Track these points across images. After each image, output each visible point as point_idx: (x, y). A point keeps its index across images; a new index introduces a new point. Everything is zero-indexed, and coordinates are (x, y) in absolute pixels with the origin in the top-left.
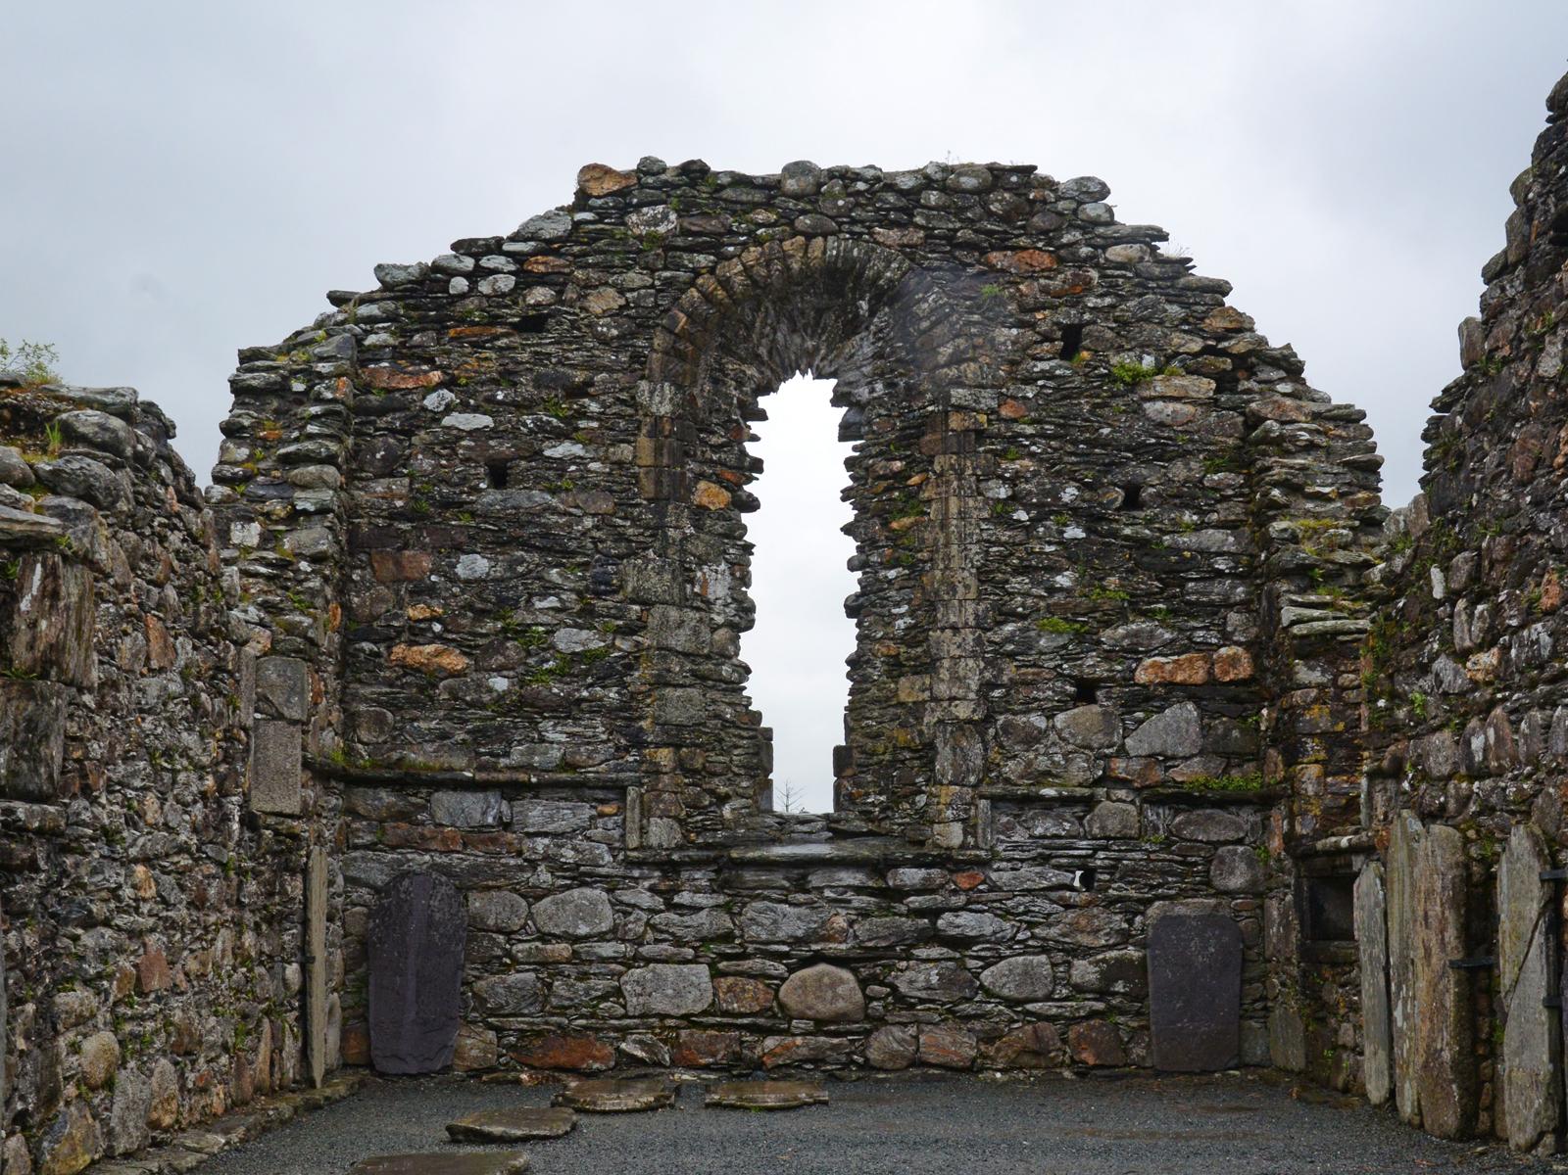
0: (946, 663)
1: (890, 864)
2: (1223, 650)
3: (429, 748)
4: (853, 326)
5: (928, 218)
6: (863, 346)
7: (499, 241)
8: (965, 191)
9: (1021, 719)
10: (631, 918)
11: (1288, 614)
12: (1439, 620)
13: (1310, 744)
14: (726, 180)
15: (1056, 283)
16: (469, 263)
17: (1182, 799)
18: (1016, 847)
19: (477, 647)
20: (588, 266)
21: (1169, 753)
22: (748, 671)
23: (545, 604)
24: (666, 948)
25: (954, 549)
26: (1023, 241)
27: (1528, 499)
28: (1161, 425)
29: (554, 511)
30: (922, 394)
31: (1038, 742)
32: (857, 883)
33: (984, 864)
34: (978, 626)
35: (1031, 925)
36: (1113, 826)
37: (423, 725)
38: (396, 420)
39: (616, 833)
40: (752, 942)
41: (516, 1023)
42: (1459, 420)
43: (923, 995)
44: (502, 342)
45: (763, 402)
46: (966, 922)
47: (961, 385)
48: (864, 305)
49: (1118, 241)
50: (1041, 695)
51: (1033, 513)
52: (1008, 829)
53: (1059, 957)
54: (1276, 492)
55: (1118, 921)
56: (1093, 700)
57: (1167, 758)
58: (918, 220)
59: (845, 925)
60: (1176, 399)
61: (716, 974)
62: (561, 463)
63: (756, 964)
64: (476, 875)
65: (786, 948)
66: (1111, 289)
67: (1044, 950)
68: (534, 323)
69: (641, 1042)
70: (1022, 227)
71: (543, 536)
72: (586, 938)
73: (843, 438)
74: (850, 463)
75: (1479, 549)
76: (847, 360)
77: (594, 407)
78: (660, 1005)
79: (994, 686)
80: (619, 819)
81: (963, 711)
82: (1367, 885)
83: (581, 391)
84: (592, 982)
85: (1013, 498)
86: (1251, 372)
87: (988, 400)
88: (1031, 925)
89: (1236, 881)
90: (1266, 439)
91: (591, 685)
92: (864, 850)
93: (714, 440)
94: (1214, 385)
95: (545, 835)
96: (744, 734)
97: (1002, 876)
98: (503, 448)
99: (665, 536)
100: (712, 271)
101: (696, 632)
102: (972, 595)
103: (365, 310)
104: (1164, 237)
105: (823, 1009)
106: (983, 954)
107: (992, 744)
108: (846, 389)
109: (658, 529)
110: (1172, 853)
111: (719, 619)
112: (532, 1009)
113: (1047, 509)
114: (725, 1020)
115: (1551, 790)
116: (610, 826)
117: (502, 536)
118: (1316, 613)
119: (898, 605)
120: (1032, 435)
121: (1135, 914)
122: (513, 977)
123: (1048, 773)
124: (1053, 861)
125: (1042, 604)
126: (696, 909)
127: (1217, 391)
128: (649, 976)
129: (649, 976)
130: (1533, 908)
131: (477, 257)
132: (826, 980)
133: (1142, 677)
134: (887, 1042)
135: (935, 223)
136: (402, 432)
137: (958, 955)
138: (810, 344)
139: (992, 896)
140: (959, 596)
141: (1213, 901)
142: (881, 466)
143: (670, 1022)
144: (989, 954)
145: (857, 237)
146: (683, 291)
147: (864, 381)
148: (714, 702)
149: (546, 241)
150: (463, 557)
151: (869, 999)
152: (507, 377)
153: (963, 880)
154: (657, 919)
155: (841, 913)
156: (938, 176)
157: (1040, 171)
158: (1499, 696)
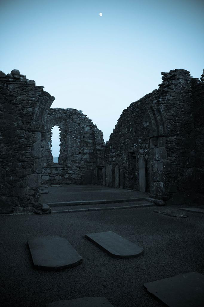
4: (61, 122)
6: (62, 124)
11: (97, 148)
13: (98, 158)
15: (78, 119)
17: (88, 162)
36: (82, 164)
45: (53, 128)
46: (70, 172)
52: (74, 164)
60: (87, 129)
61: (50, 176)
63: (53, 176)
66: (82, 120)
67: (76, 174)
74: (60, 133)
78: (45, 179)
81: (70, 155)
85: (74, 137)
89: (91, 169)
90: (95, 133)
100: (50, 117)
104: (87, 116)
113: (77, 138)
126: (48, 171)
130: (118, 171)
133: (84, 152)
134: (64, 182)
145: (62, 114)
155: (60, 171)
157: (77, 110)
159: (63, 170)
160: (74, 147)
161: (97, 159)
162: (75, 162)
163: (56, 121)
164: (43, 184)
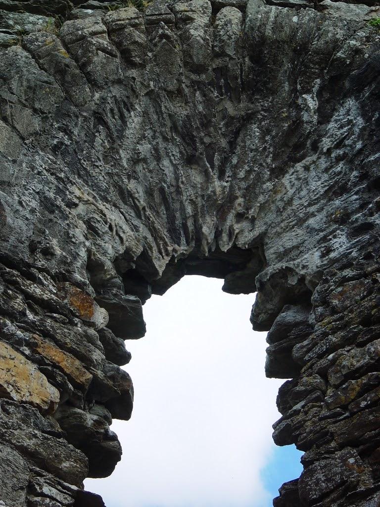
4: (294, 146)
76: (279, 212)
108: (279, 266)
163: (188, 138)
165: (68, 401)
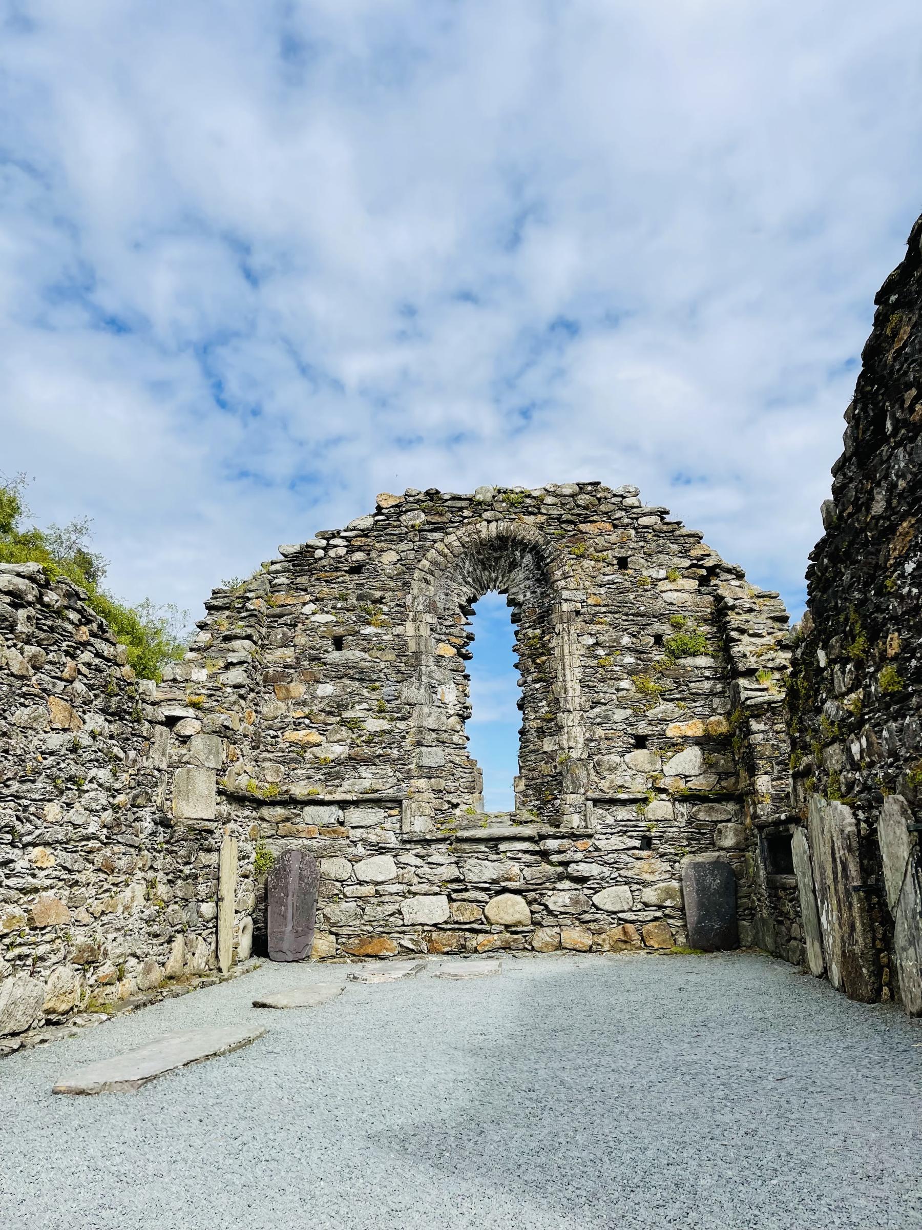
0: (566, 730)
1: (542, 837)
2: (712, 718)
3: (303, 783)
4: (513, 565)
5: (548, 510)
6: (519, 575)
7: (338, 533)
8: (565, 496)
9: (606, 758)
10: (406, 871)
11: (744, 695)
12: (824, 679)
14: (447, 497)
15: (613, 538)
16: (324, 543)
18: (608, 826)
19: (326, 731)
20: (382, 541)
21: (687, 774)
22: (468, 739)
23: (361, 707)
24: (425, 887)
25: (568, 671)
26: (595, 518)
27: (873, 592)
28: (672, 604)
29: (364, 660)
30: (549, 595)
31: (616, 769)
32: (524, 848)
33: (590, 836)
34: (581, 710)
35: (618, 869)
37: (299, 772)
38: (287, 619)
39: (398, 825)
40: (470, 882)
41: (345, 931)
42: (826, 561)
43: (562, 910)
44: (340, 580)
46: (584, 869)
47: (567, 589)
48: (518, 553)
49: (644, 515)
50: (616, 745)
51: (607, 651)
53: (635, 887)
54: (732, 633)
55: (666, 866)
56: (644, 747)
57: (686, 777)
58: (543, 511)
59: (519, 872)
60: (680, 593)
61: (451, 900)
62: (367, 638)
63: (471, 895)
64: (325, 850)
65: (487, 885)
68: (356, 569)
69: (412, 940)
70: (595, 511)
71: (361, 673)
72: (382, 883)
73: (513, 622)
75: (844, 631)
77: (386, 609)
79: (592, 741)
80: (399, 817)
81: (575, 755)
82: (798, 842)
83: (380, 601)
84: (386, 906)
85: (597, 644)
86: (717, 575)
87: (580, 595)
88: (618, 869)
89: (729, 841)
91: (384, 748)
92: (527, 831)
93: (447, 623)
94: (697, 583)
95: (362, 827)
96: (466, 771)
97: (601, 844)
98: (340, 630)
99: (420, 670)
101: (438, 718)
102: (578, 693)
103: (273, 568)
104: (667, 513)
105: (509, 920)
106: (592, 886)
107: (592, 772)
109: (417, 666)
110: (693, 827)
111: (452, 712)
112: (354, 923)
113: (614, 649)
114: (457, 926)
115: (908, 771)
116: (395, 821)
117: (340, 674)
118: (759, 693)
119: (541, 701)
120: (605, 612)
121: (675, 862)
122: (344, 905)
123: (622, 786)
124: (629, 834)
125: (614, 697)
127: (700, 585)
128: (415, 903)
129: (415, 903)
131: (328, 539)
132: (509, 902)
134: (543, 936)
135: (551, 512)
136: (291, 625)
137: (579, 887)
138: (493, 575)
139: (596, 854)
140: (570, 694)
141: (717, 854)
142: (530, 632)
143: (426, 928)
144: (596, 886)
146: (428, 551)
147: (521, 592)
148: (450, 754)
149: (362, 530)
150: (320, 685)
151: (532, 912)
152: (344, 598)
153: (580, 845)
154: (419, 871)
156: (552, 489)
158: (867, 717)
159: (533, 853)
160: (596, 704)
161: (752, 771)
162: (613, 802)
163: (483, 564)
164: (412, 950)
165: (458, 650)
